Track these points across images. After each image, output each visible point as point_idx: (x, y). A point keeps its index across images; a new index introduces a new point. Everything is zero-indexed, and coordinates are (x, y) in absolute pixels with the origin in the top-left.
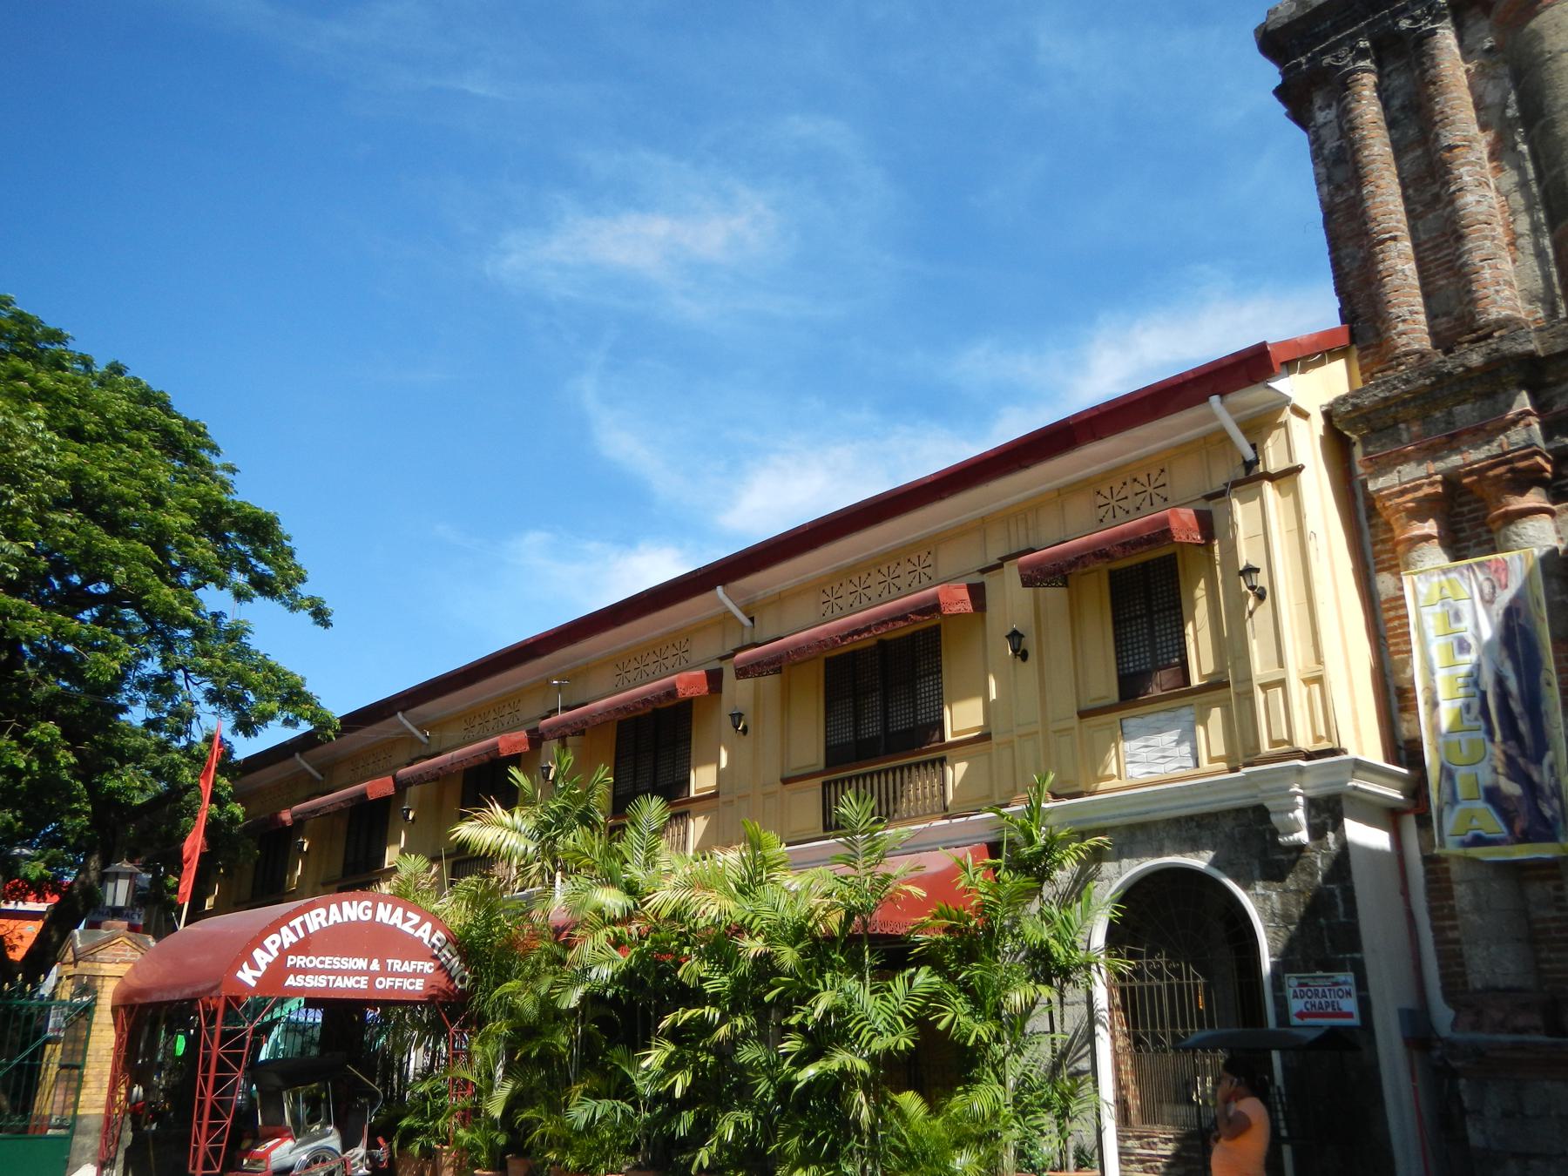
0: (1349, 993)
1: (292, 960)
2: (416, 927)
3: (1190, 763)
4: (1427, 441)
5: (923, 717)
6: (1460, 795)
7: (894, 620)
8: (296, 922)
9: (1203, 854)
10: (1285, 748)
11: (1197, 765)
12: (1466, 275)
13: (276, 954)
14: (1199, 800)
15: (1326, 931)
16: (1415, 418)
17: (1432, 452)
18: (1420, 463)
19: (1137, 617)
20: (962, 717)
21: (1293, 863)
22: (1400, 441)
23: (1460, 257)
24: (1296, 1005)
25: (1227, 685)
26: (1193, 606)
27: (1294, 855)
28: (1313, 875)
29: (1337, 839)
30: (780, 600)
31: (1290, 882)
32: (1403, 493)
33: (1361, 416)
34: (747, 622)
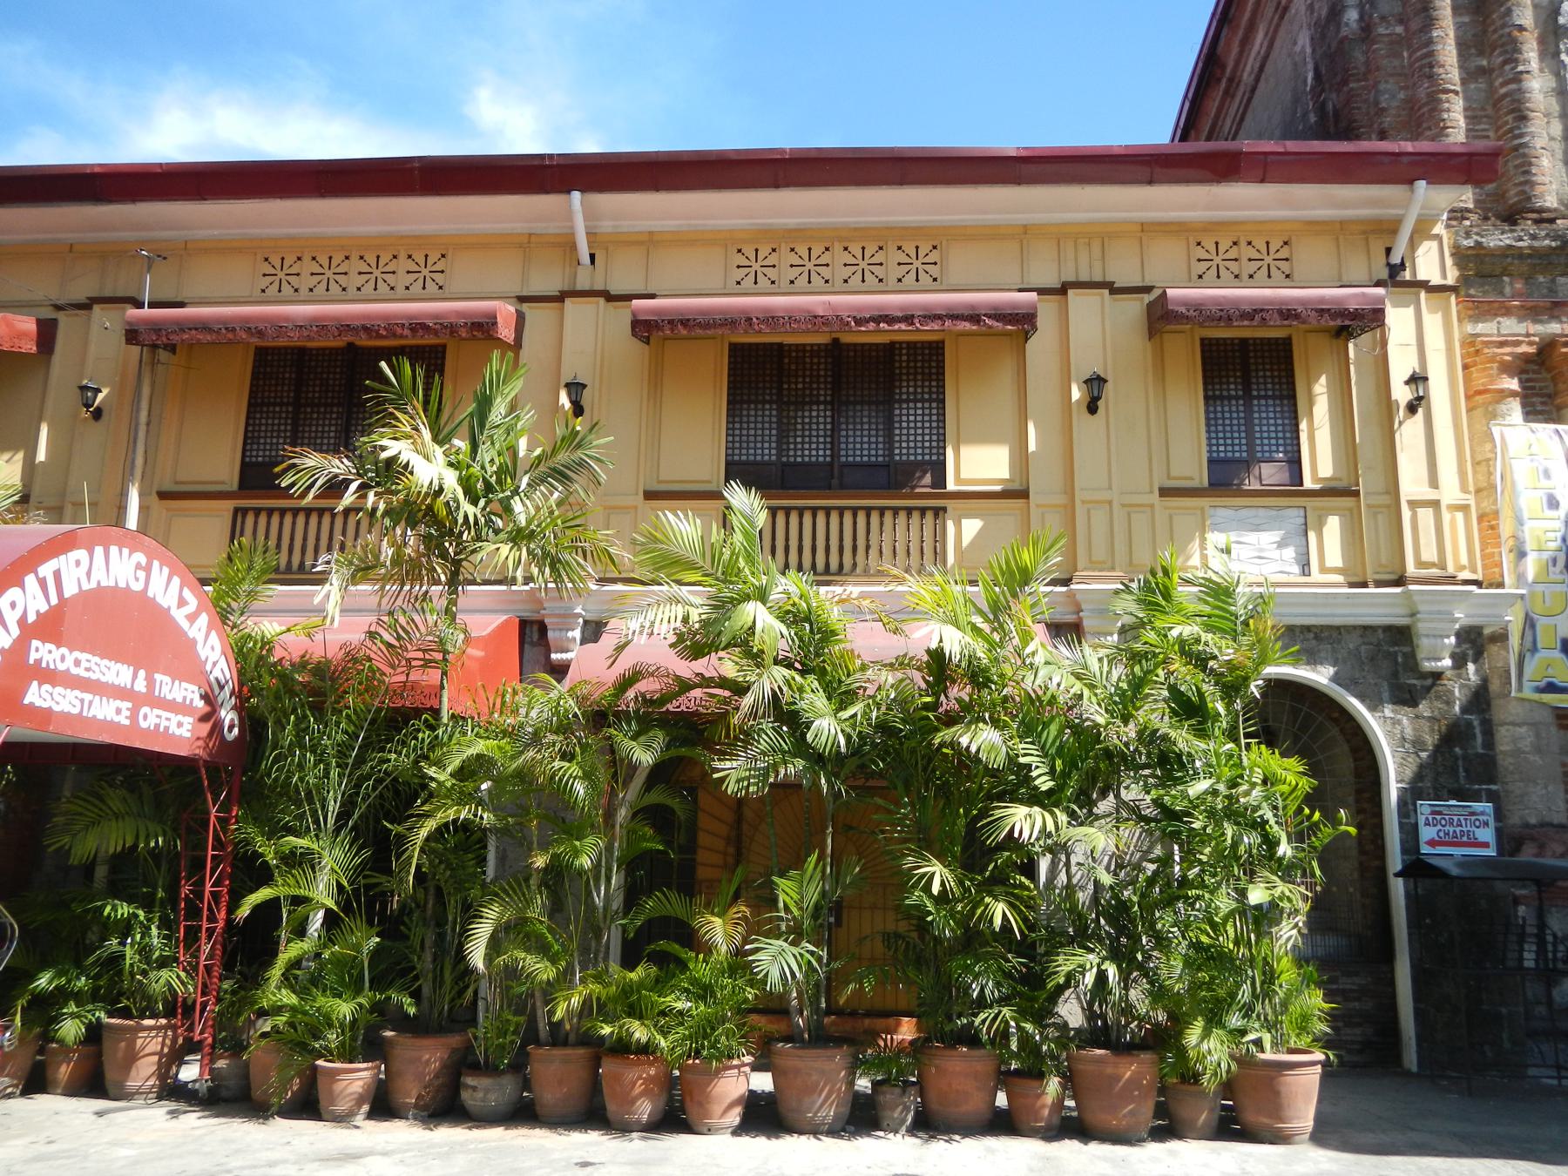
0: (1486, 824)
1: (43, 652)
2: (192, 618)
3: (1296, 569)
4: (1536, 300)
5: (902, 453)
6: (1539, 645)
7: (955, 317)
8: (46, 570)
9: (1320, 668)
10: (1435, 572)
11: (1305, 568)
12: (1524, 155)
13: (15, 631)
14: (1328, 611)
15: (1461, 761)
16: (1521, 275)
17: (1533, 313)
18: (1521, 319)
19: (1230, 398)
20: (978, 463)
21: (1428, 689)
22: (1502, 293)
23: (1521, 136)
24: (1427, 833)
25: (1356, 494)
26: (1311, 403)
27: (1429, 682)
28: (1449, 703)
29: (1477, 671)
30: (650, 242)
31: (1424, 708)
32: (1502, 344)
33: (1477, 256)
34: (586, 259)
